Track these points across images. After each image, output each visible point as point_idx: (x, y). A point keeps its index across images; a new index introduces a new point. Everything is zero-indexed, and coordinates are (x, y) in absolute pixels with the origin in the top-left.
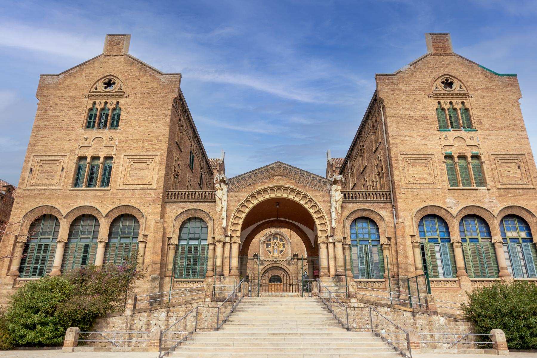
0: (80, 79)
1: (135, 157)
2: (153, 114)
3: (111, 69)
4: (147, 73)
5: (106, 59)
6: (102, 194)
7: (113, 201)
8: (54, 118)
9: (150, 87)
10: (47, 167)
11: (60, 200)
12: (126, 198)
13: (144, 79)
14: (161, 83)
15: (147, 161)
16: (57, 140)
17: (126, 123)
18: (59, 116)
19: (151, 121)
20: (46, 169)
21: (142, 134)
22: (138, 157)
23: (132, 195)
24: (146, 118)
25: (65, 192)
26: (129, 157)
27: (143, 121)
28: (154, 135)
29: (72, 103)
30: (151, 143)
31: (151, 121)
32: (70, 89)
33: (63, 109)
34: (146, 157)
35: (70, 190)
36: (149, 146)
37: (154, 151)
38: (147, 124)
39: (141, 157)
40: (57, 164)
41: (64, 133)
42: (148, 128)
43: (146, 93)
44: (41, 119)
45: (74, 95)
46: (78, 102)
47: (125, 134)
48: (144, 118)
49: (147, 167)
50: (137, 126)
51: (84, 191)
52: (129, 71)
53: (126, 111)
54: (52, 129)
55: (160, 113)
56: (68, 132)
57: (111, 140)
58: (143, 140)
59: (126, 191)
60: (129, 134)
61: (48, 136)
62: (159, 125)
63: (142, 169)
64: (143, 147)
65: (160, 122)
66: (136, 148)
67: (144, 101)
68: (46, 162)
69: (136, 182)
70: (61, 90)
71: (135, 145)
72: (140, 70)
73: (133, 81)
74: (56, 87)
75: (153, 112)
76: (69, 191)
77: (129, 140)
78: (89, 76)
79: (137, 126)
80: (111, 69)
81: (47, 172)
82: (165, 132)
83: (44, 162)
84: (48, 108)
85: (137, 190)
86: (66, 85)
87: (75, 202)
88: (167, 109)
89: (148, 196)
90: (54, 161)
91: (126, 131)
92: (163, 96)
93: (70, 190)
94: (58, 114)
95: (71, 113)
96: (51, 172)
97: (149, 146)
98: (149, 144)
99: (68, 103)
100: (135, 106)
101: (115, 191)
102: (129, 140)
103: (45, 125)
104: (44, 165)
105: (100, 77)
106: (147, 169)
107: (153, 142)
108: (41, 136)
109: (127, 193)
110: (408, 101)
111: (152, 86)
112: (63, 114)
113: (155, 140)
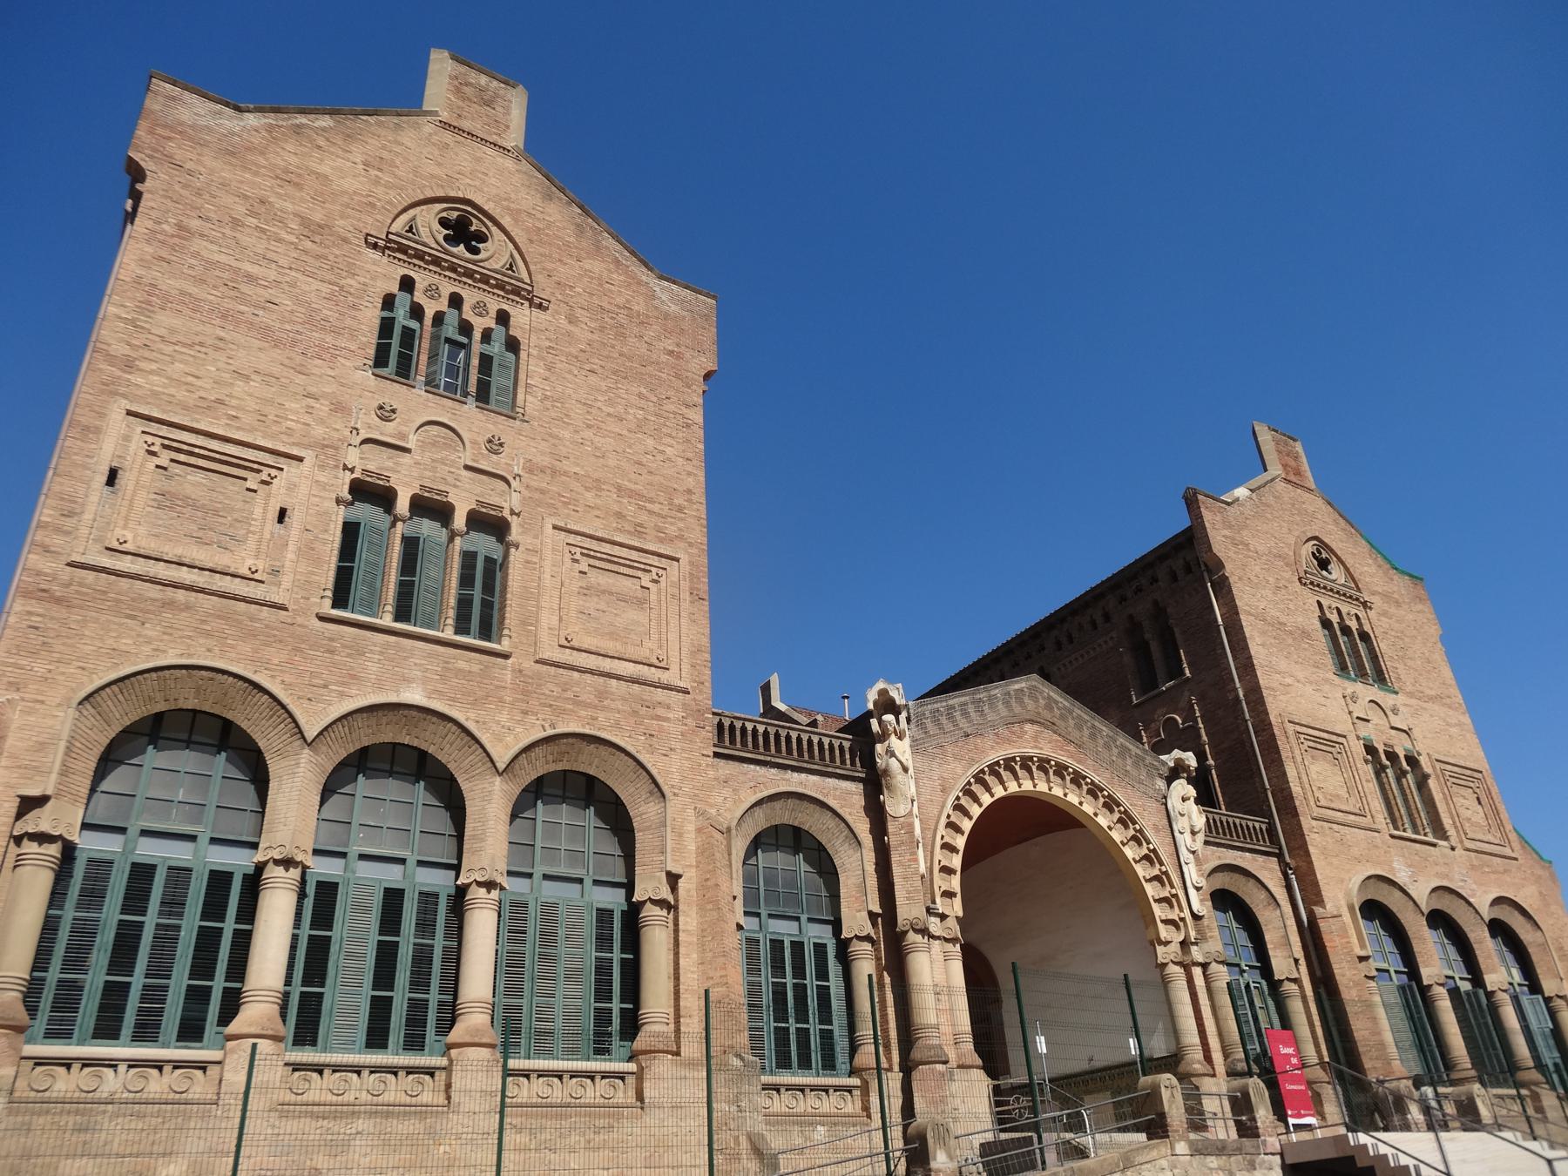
1: (594, 545)
2: (643, 403)
3: (468, 181)
5: (448, 137)
6: (476, 668)
7: (524, 706)
8: (226, 275)
9: (620, 301)
10: (193, 482)
11: (276, 656)
12: (577, 702)
15: (639, 574)
16: (248, 378)
17: (548, 404)
18: (251, 278)
19: (640, 426)
20: (189, 490)
22: (607, 548)
23: (602, 695)
25: (299, 620)
26: (572, 539)
28: (657, 479)
29: (308, 245)
31: (640, 426)
33: (270, 255)
34: (634, 555)
35: (322, 618)
37: (661, 541)
38: (625, 432)
39: (617, 551)
40: (251, 484)
41: (276, 354)
42: (630, 447)
45: (318, 216)
47: (544, 444)
48: (612, 405)
49: (640, 593)
50: (589, 426)
51: (393, 639)
54: (217, 322)
55: (665, 408)
56: (299, 359)
57: (496, 453)
58: (619, 488)
59: (576, 674)
60: (564, 451)
61: (201, 344)
62: (669, 450)
63: (623, 599)
65: (669, 440)
66: (597, 513)
68: (193, 460)
69: (610, 646)
70: (256, 174)
73: (556, 256)
75: (640, 395)
76: (319, 624)
78: (380, 170)
79: (589, 426)
80: (468, 181)
81: (195, 507)
83: (182, 457)
84: (195, 224)
85: (619, 678)
87: (353, 677)
89: (660, 711)
90: (233, 467)
91: (551, 435)
92: (671, 353)
93: (322, 618)
94: (248, 267)
95: (311, 286)
96: (216, 513)
97: (643, 517)
98: (641, 508)
100: (574, 351)
101: (528, 664)
102: (565, 474)
103: (183, 293)
104: (177, 469)
105: (429, 194)
106: (641, 603)
107: (656, 508)
108: (162, 332)
109: (578, 684)
110: (1267, 582)
112: (272, 274)
113: (662, 500)
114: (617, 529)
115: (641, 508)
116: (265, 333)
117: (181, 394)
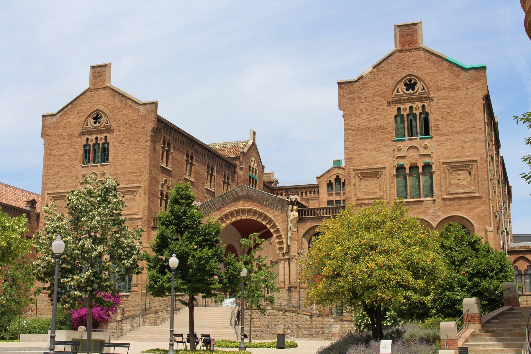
0: (73, 116)
3: (97, 103)
4: (127, 105)
5: (93, 93)
8: (57, 157)
9: (131, 118)
13: (125, 111)
14: (140, 114)
18: (61, 155)
21: (127, 167)
24: (130, 151)
27: (127, 154)
28: (137, 167)
30: (135, 174)
32: (66, 127)
36: (135, 178)
37: (138, 183)
38: (131, 157)
43: (128, 126)
44: (48, 159)
45: (70, 133)
46: (74, 140)
49: (134, 197)
50: (123, 159)
52: (112, 103)
53: (113, 145)
56: (69, 169)
58: (129, 173)
62: (141, 157)
64: (129, 180)
66: (124, 181)
67: (127, 134)
71: (123, 178)
72: (122, 101)
73: (116, 114)
74: (55, 127)
75: (135, 145)
77: (118, 174)
79: (123, 159)
82: (146, 163)
86: (63, 123)
88: (147, 140)
91: (115, 165)
94: (60, 153)
97: (135, 178)
99: (67, 141)
100: (120, 139)
102: (118, 174)
103: (52, 164)
106: (134, 199)
107: (137, 174)
111: (133, 117)
112: (64, 152)
114: (129, 184)
115: (133, 176)
116: (64, 166)
117: (54, 186)
